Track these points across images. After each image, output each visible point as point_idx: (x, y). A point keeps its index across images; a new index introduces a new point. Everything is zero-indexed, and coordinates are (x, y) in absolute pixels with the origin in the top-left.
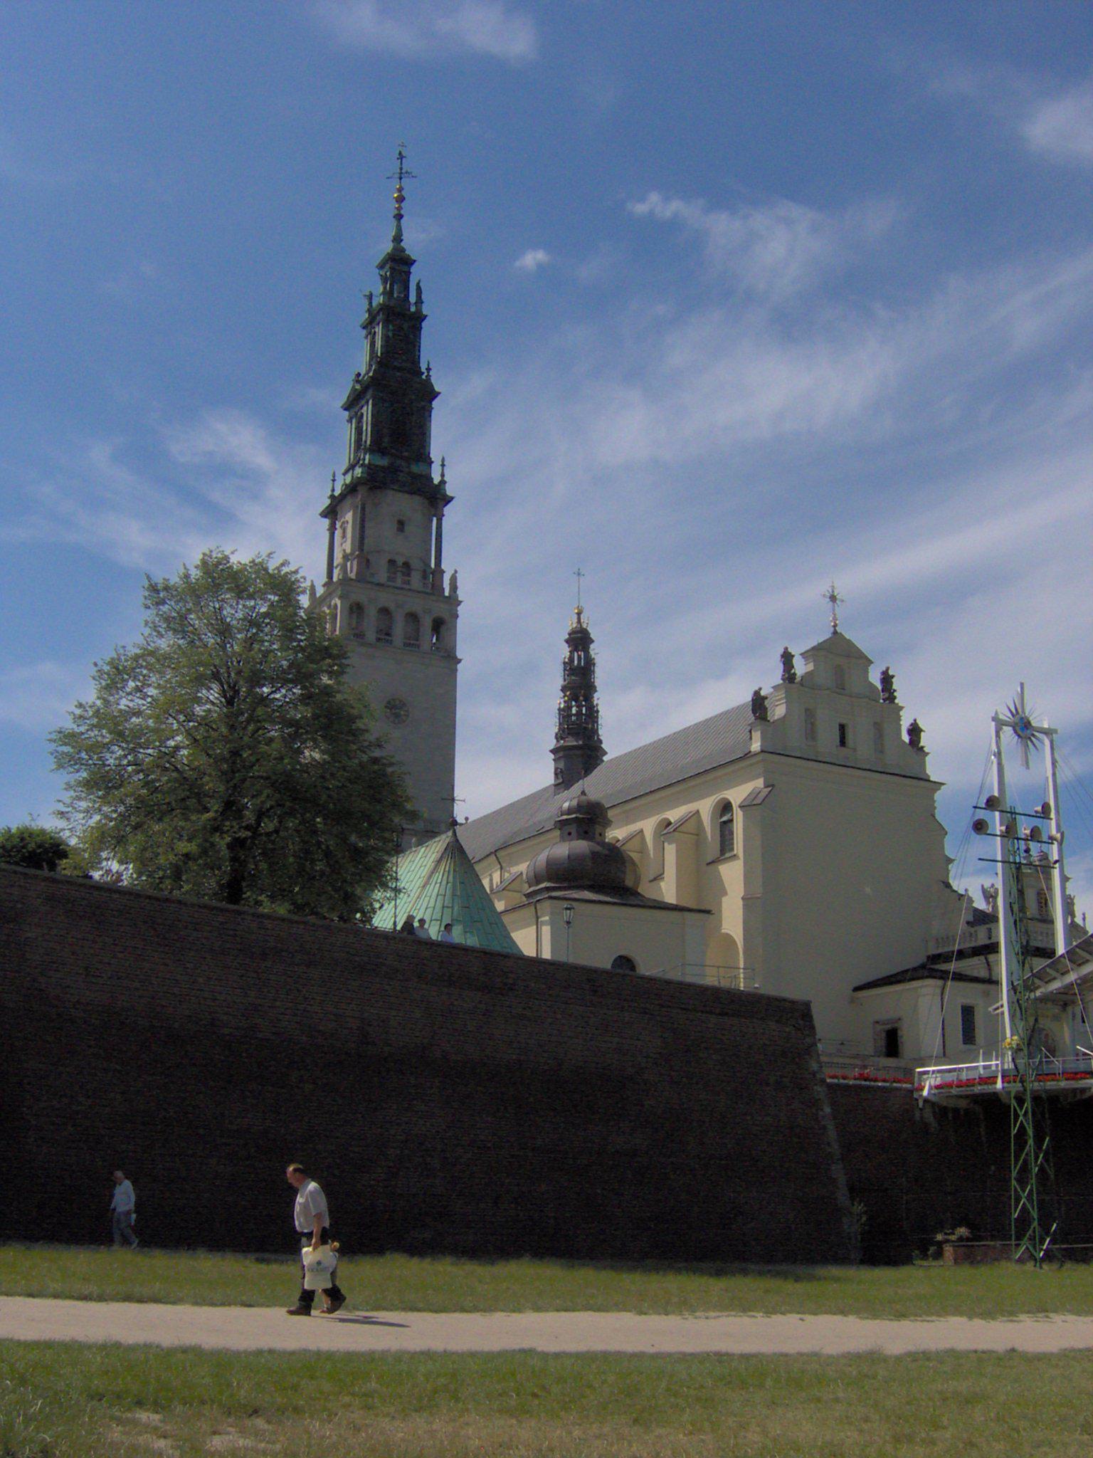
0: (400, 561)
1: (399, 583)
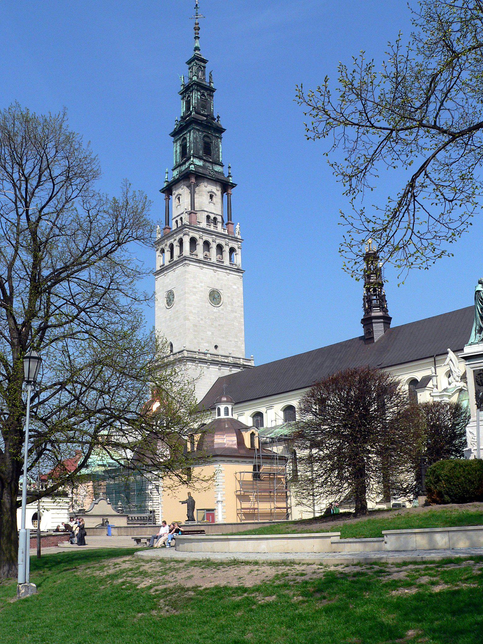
0: (212, 216)
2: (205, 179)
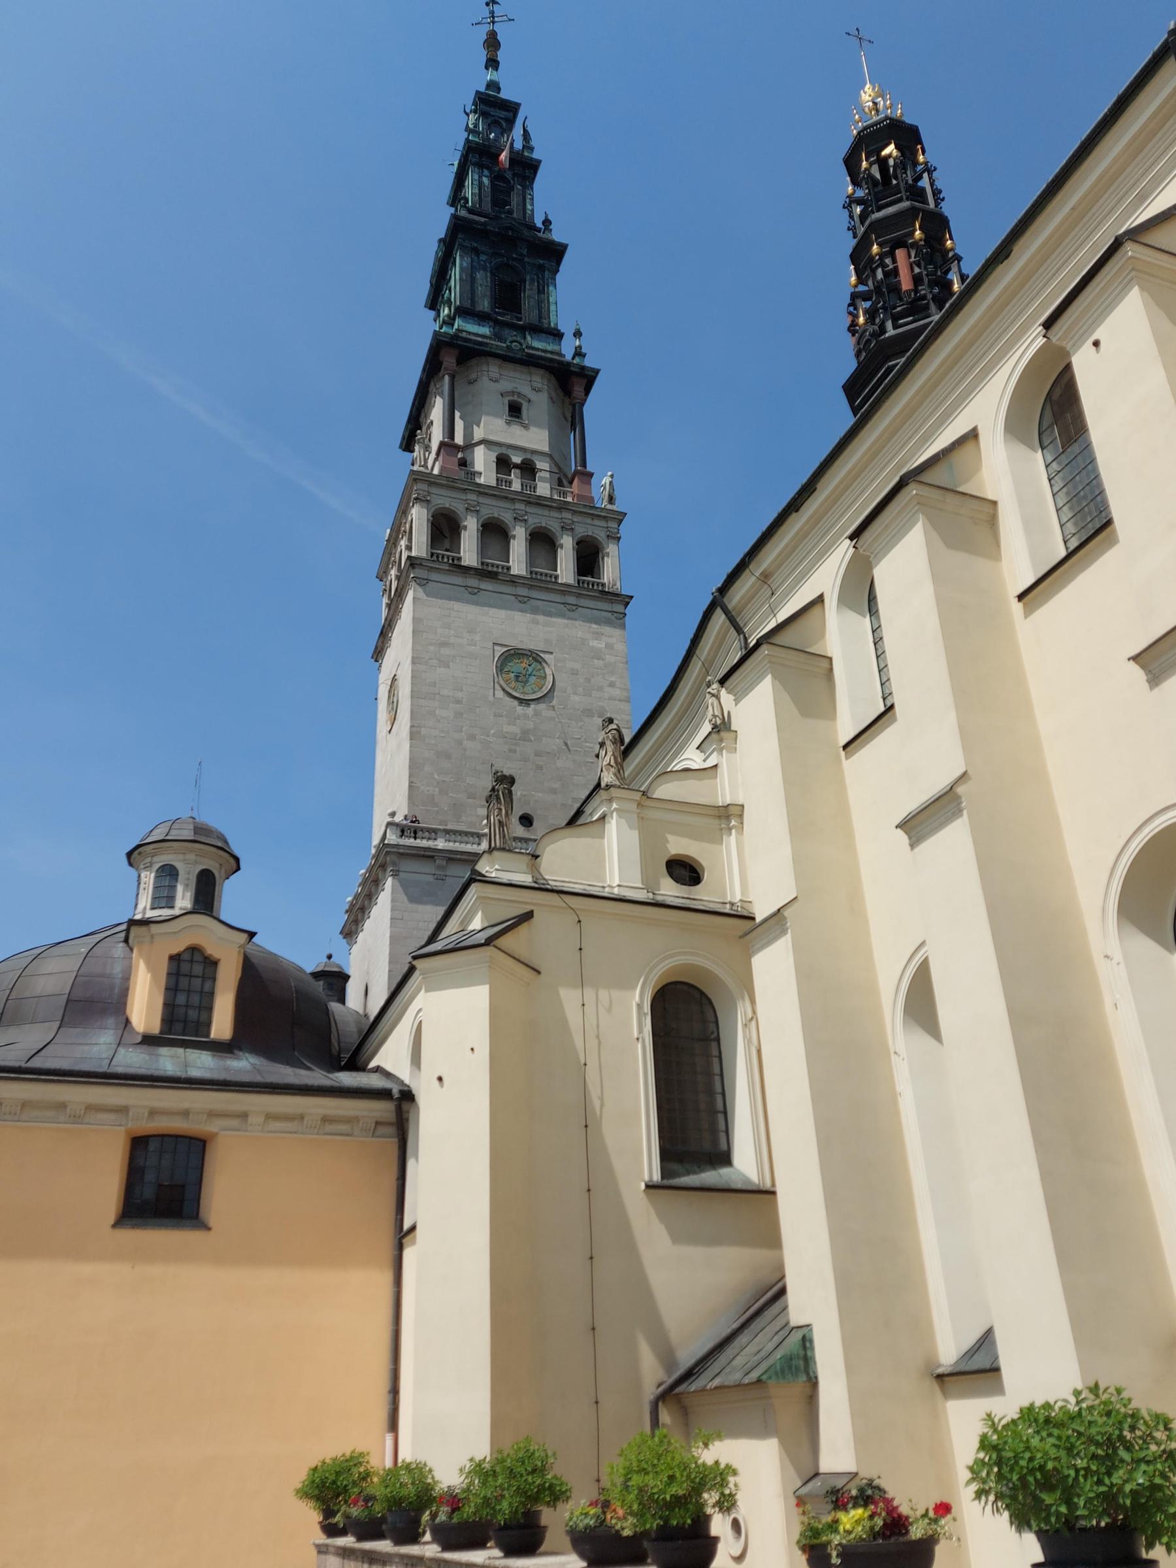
0: (517, 459)
1: (516, 486)
2: (491, 360)
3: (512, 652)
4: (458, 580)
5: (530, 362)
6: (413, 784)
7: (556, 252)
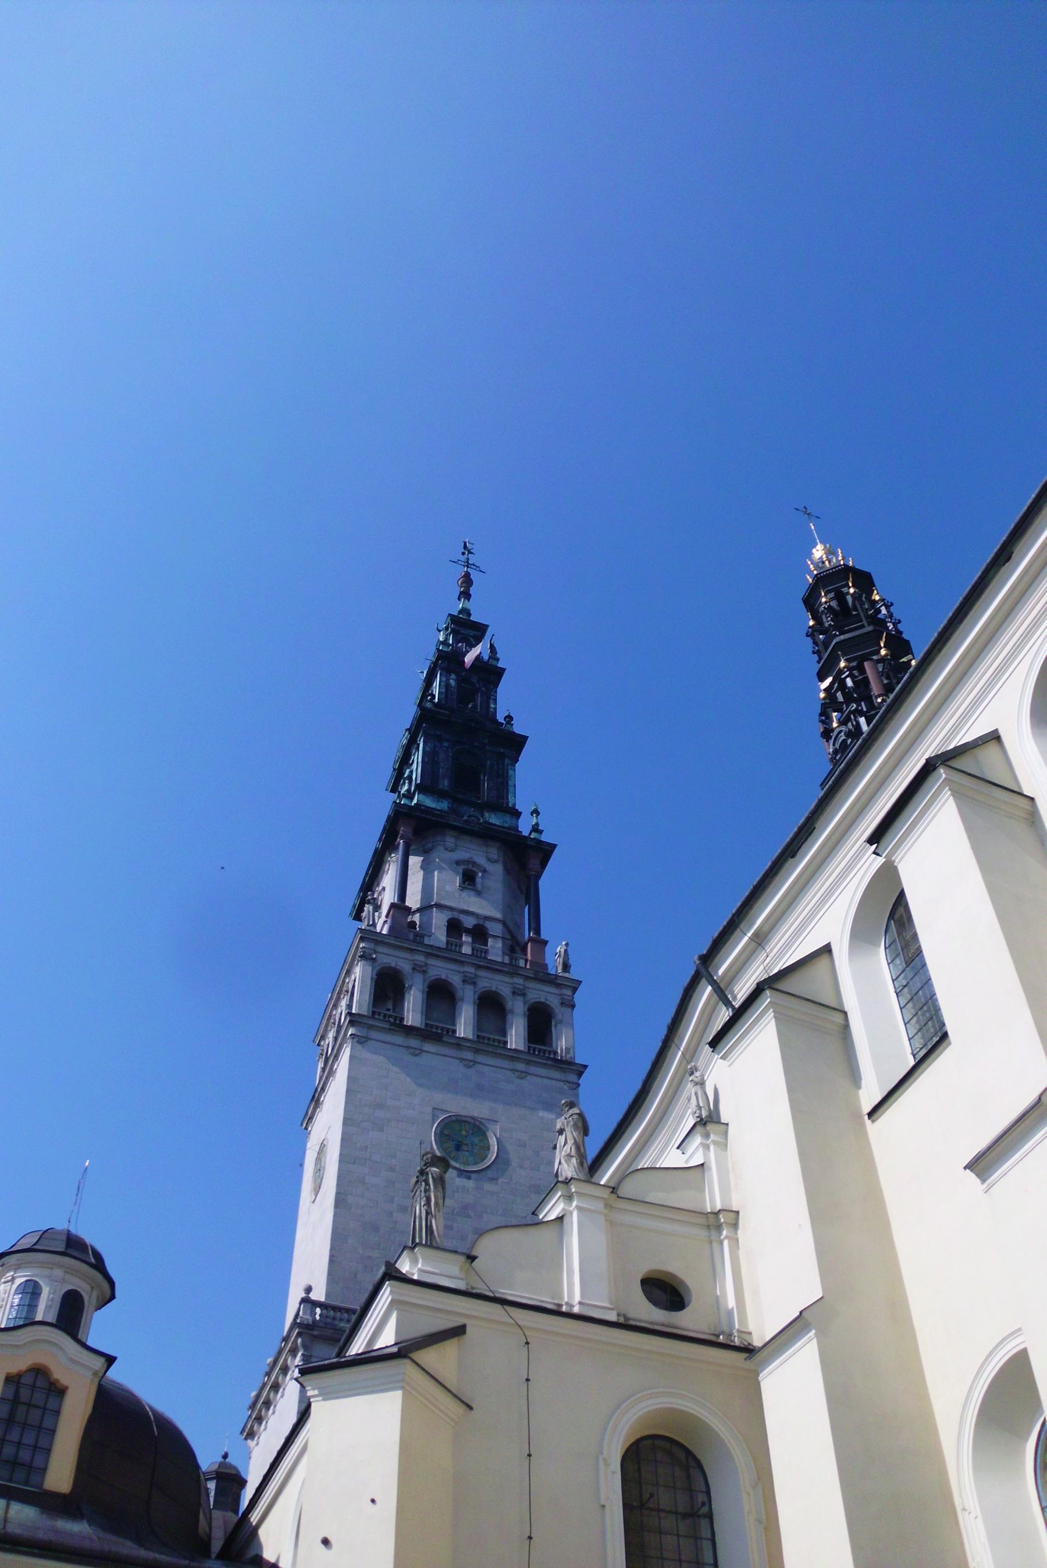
0: (469, 922)
3: (454, 1118)
4: (399, 1039)
5: (486, 835)
6: (334, 1259)
7: (518, 743)
